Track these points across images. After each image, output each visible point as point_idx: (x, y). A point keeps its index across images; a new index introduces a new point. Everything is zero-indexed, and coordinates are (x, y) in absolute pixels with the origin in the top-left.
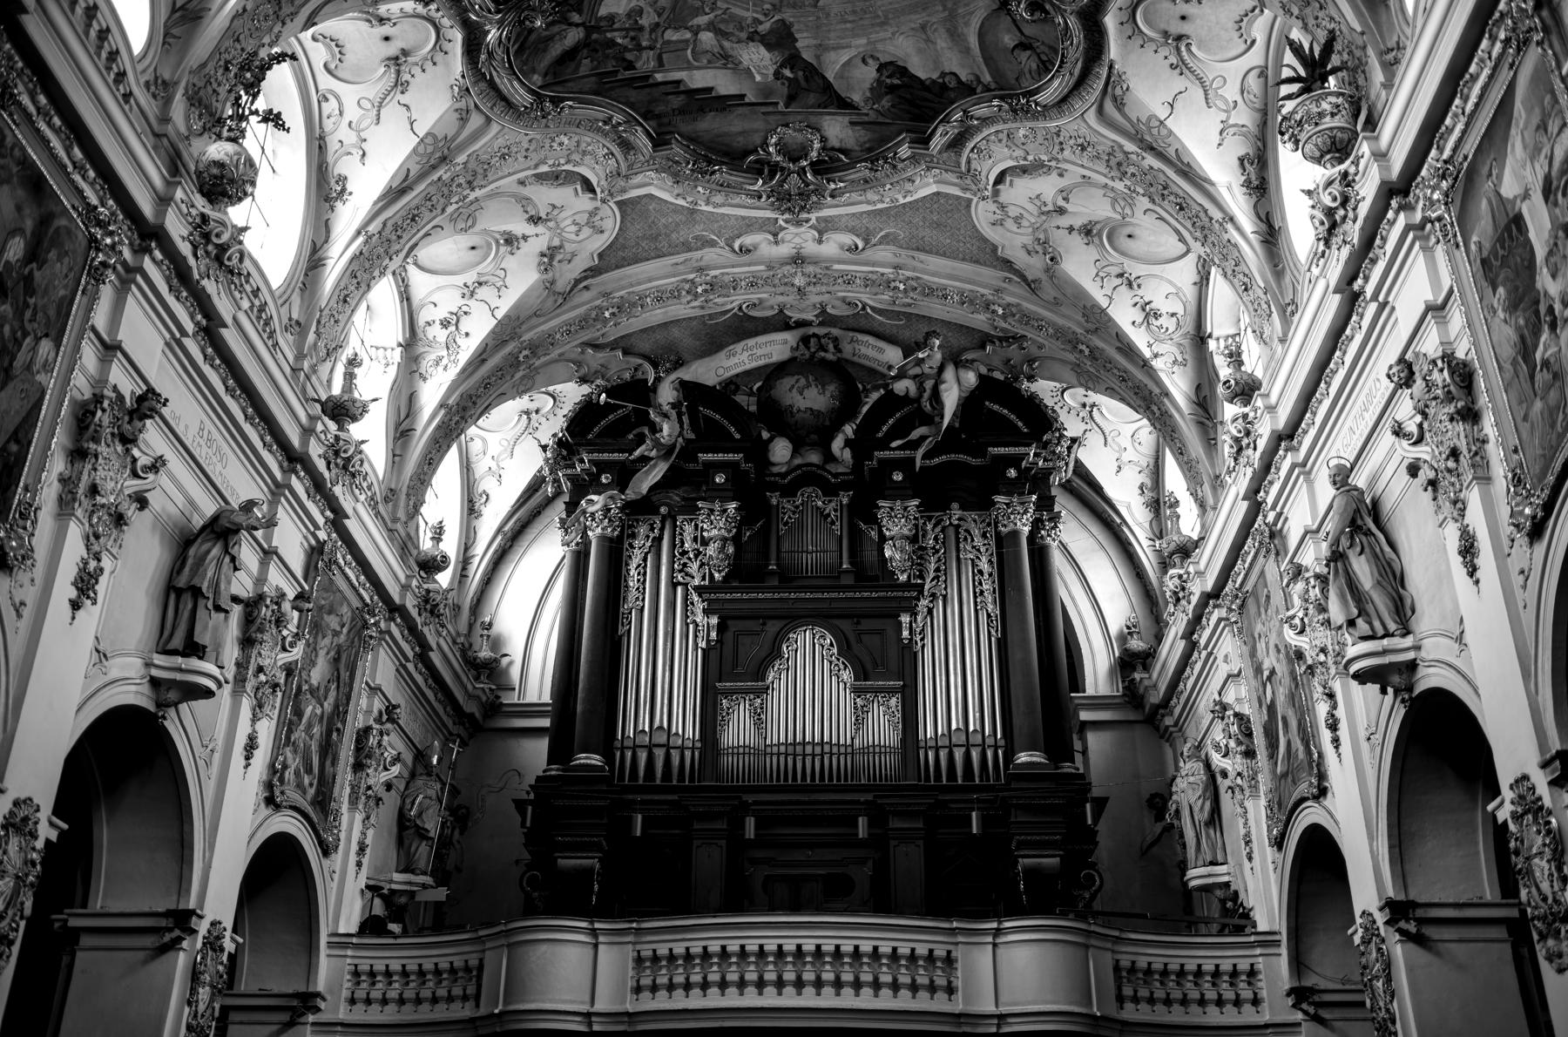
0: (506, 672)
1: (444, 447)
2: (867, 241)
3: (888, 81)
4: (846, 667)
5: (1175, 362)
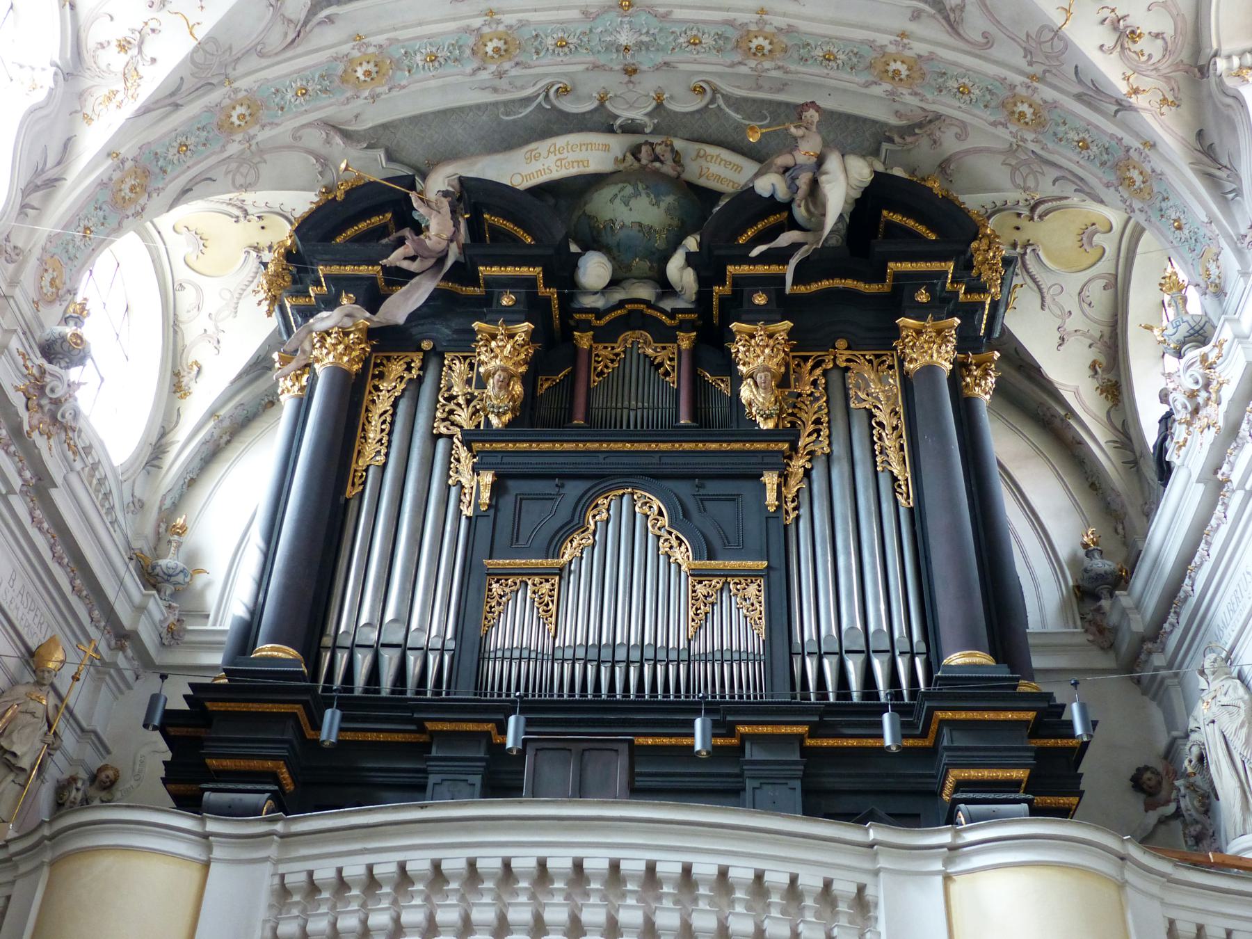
0: (201, 595)
1: (111, 221)
4: (681, 542)
5: (1165, 99)
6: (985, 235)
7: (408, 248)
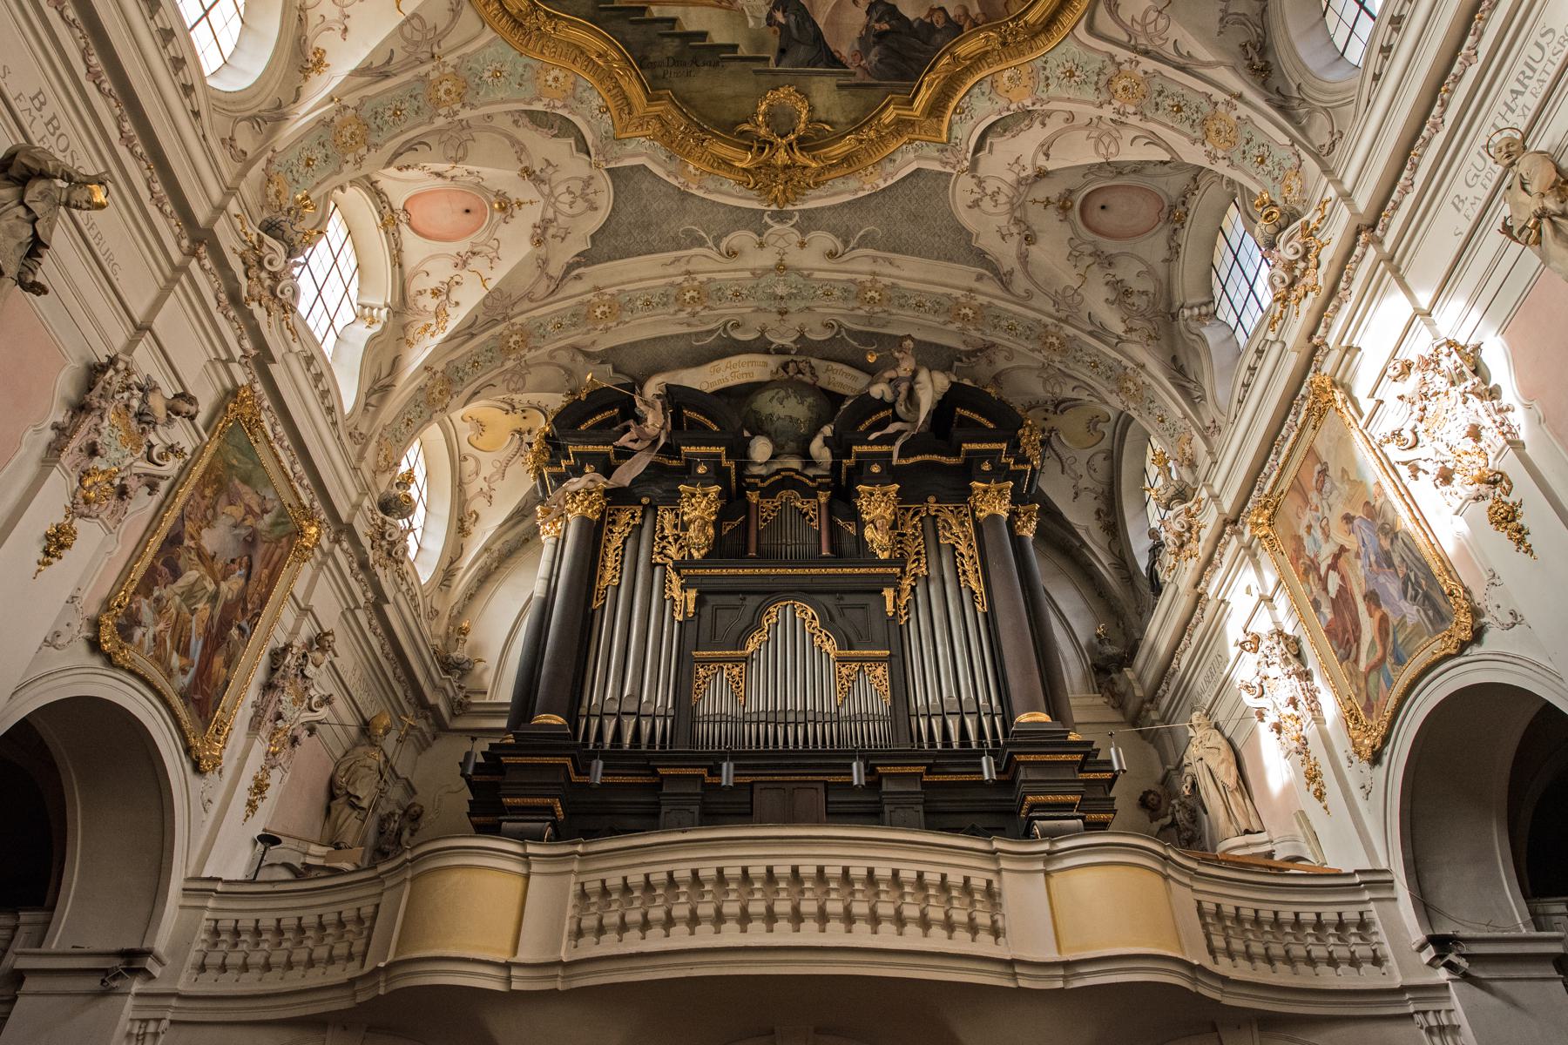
1: (426, 415)
2: (846, 243)
3: (877, 26)
4: (829, 638)
6: (1028, 425)
7: (633, 434)
